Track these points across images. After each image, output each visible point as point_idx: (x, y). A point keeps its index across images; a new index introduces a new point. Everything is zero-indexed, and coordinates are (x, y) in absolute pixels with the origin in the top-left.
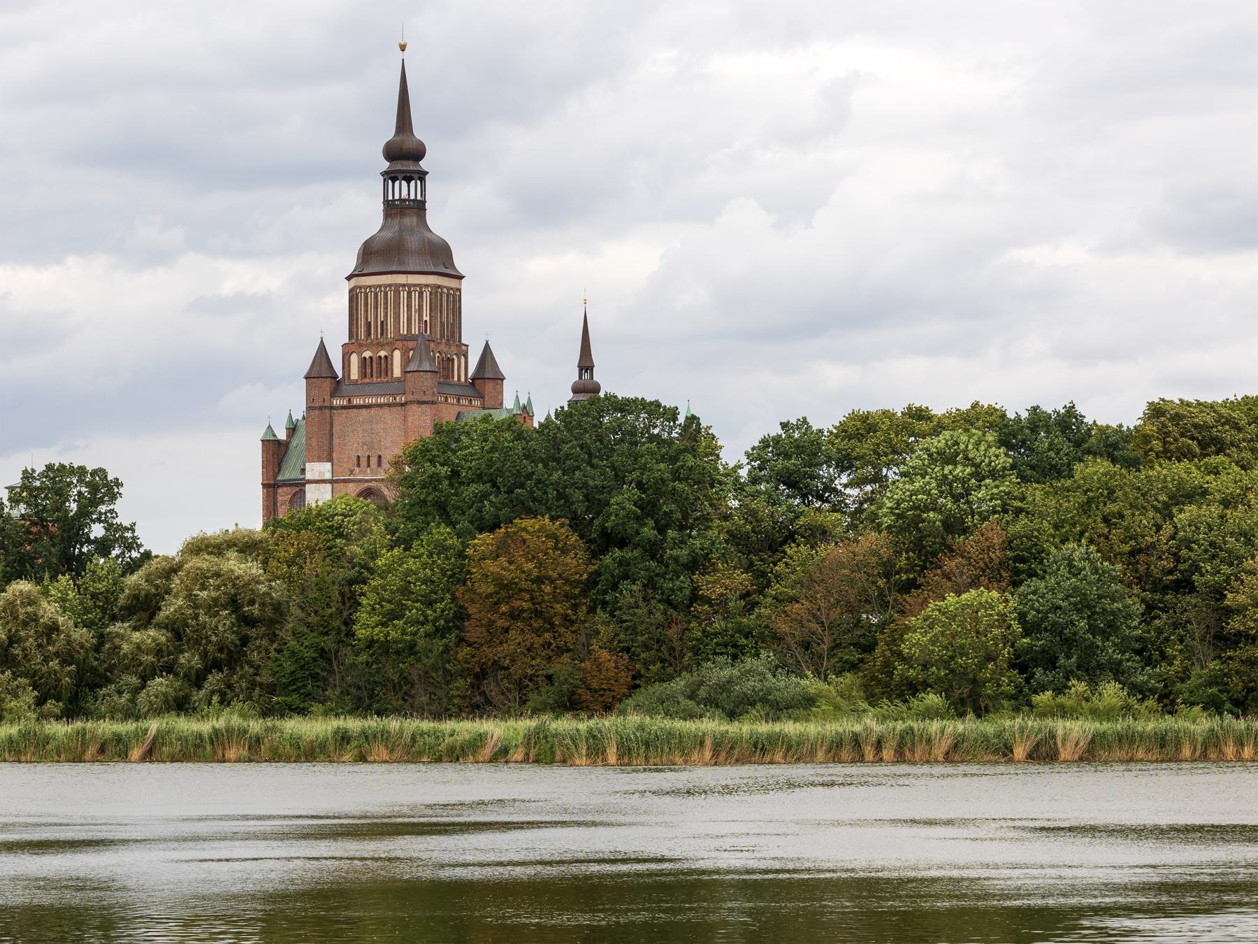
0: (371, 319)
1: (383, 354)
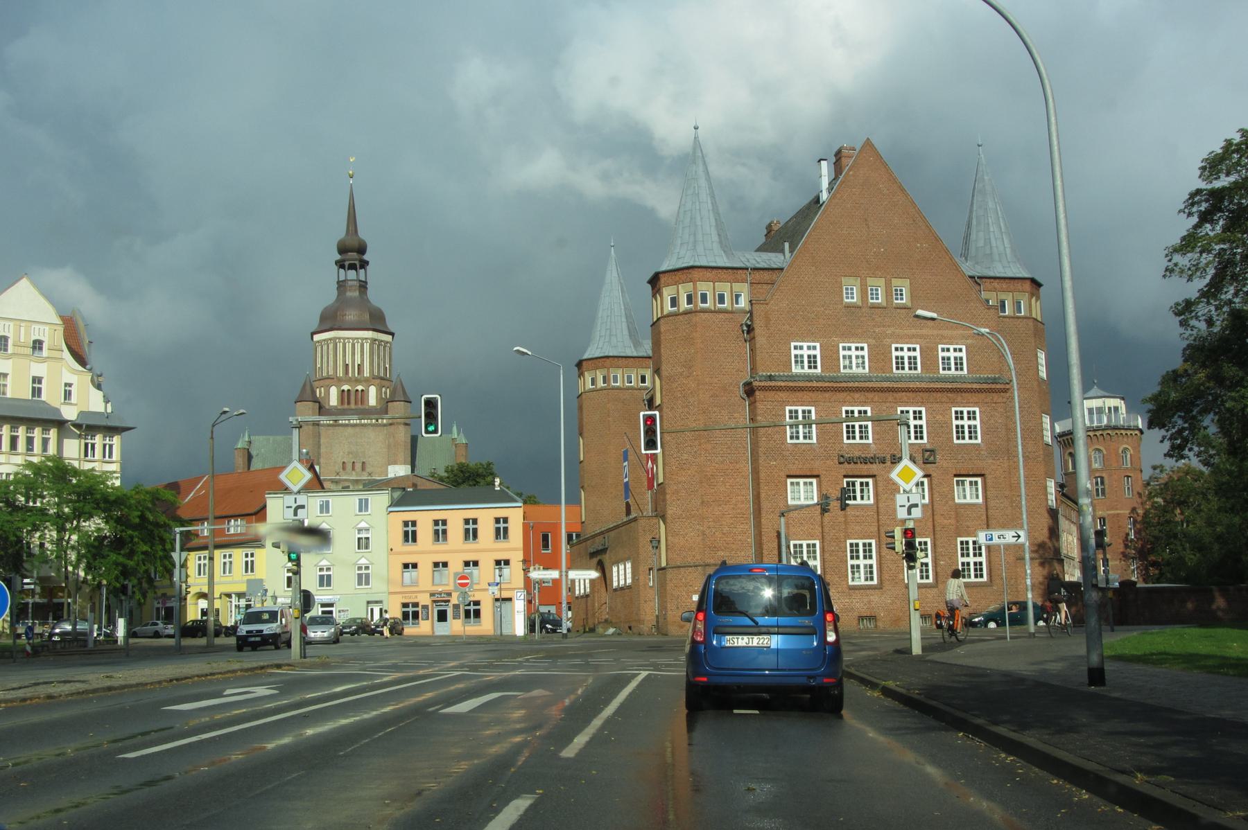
0: (349, 361)
1: (360, 388)
